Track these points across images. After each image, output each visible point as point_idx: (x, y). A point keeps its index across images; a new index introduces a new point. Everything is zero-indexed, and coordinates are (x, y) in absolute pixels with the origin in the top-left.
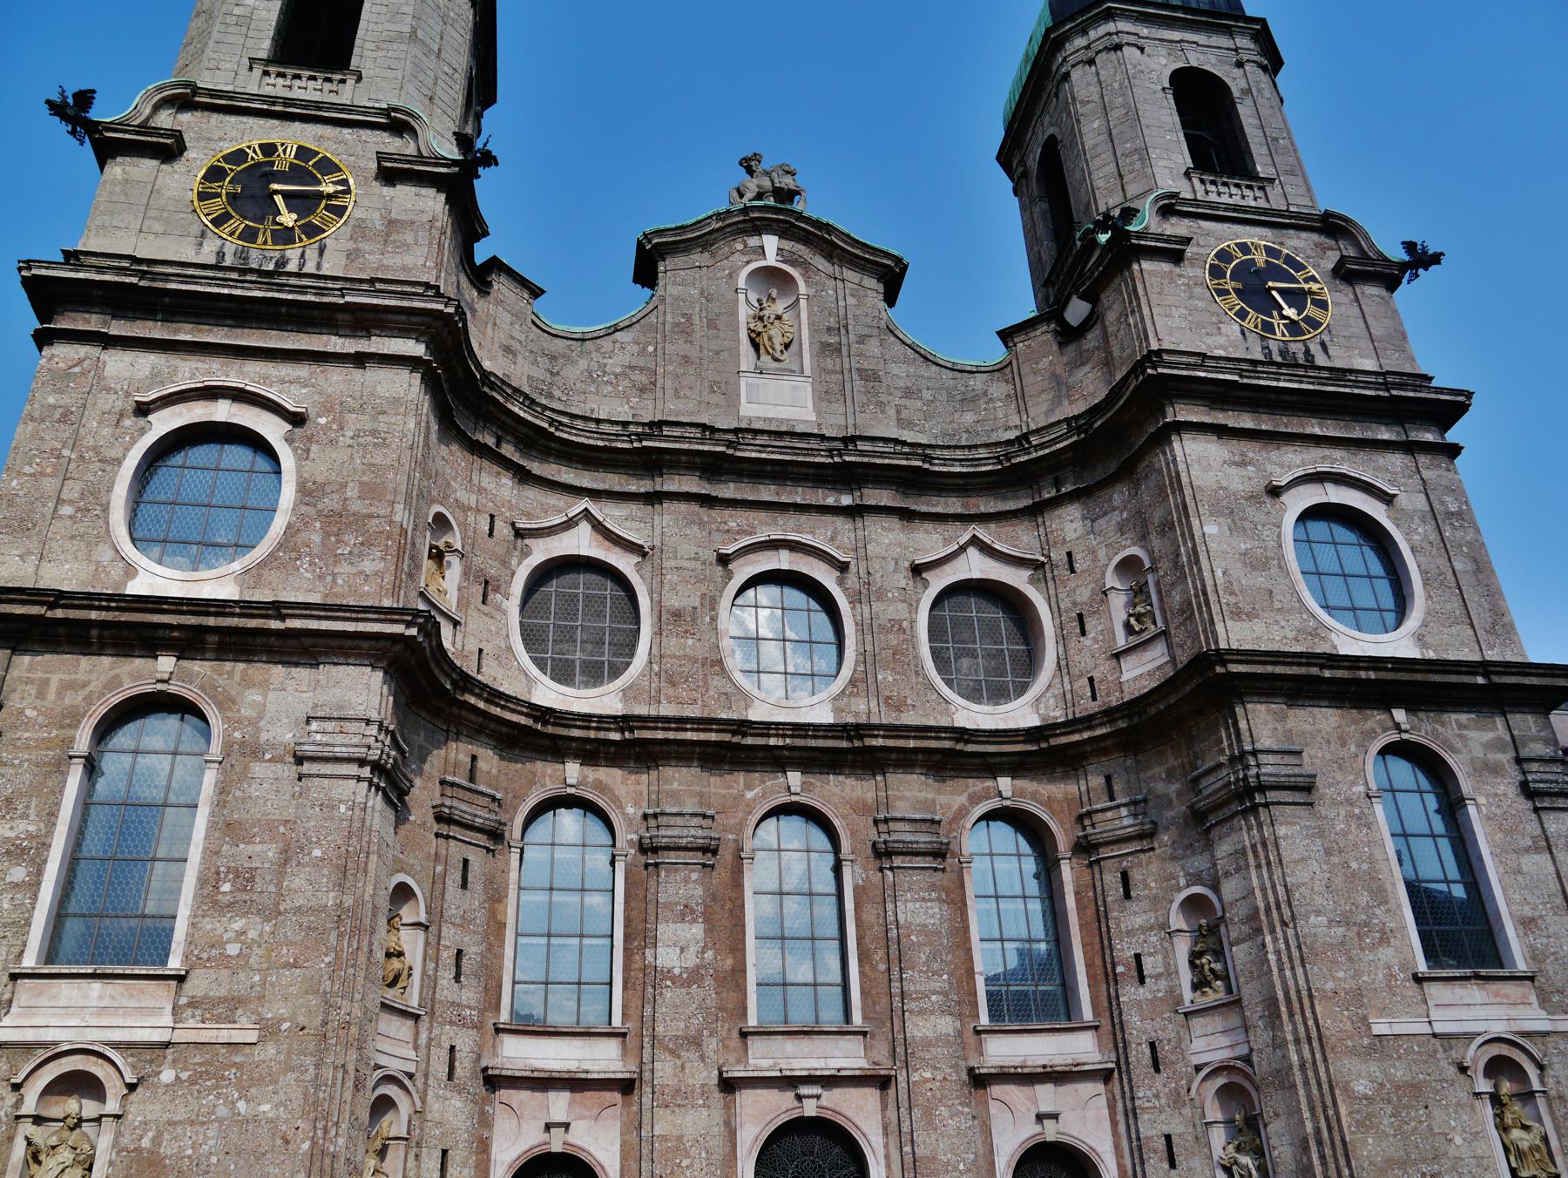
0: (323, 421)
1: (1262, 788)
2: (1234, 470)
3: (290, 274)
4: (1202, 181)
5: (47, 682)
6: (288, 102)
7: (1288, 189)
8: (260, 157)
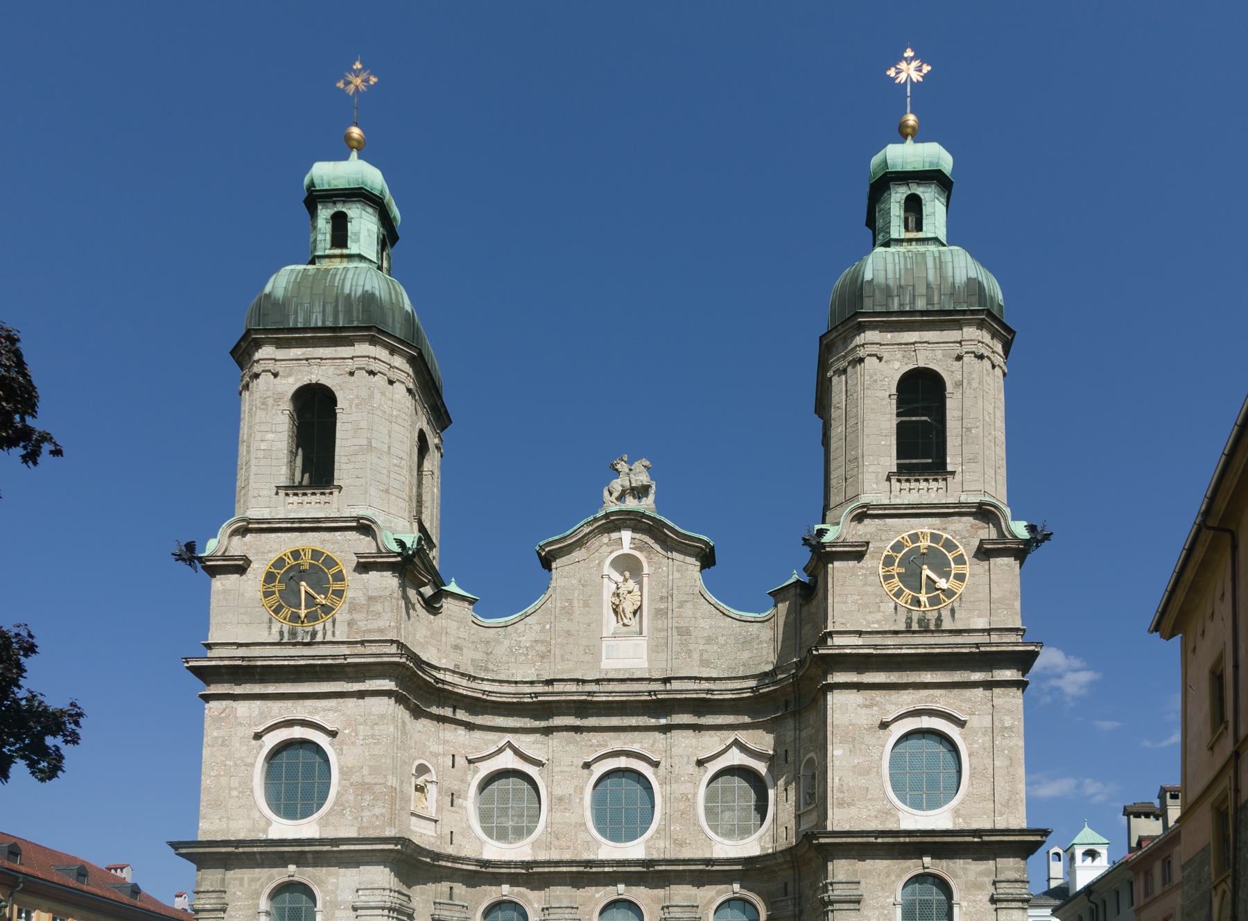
0: (347, 731)
1: (831, 903)
2: (864, 711)
3: (319, 643)
4: (899, 481)
5: (242, 879)
6: (302, 520)
7: (967, 476)
8: (293, 562)
